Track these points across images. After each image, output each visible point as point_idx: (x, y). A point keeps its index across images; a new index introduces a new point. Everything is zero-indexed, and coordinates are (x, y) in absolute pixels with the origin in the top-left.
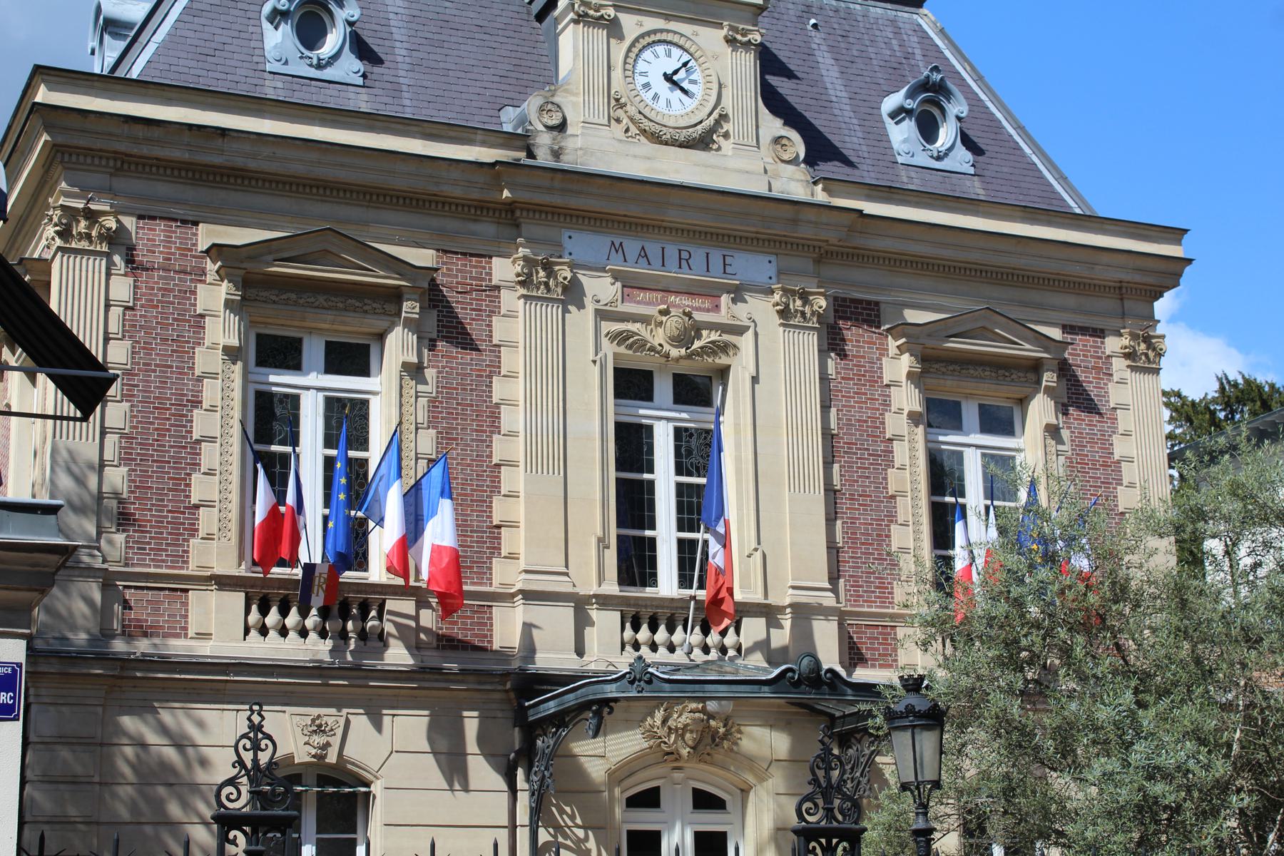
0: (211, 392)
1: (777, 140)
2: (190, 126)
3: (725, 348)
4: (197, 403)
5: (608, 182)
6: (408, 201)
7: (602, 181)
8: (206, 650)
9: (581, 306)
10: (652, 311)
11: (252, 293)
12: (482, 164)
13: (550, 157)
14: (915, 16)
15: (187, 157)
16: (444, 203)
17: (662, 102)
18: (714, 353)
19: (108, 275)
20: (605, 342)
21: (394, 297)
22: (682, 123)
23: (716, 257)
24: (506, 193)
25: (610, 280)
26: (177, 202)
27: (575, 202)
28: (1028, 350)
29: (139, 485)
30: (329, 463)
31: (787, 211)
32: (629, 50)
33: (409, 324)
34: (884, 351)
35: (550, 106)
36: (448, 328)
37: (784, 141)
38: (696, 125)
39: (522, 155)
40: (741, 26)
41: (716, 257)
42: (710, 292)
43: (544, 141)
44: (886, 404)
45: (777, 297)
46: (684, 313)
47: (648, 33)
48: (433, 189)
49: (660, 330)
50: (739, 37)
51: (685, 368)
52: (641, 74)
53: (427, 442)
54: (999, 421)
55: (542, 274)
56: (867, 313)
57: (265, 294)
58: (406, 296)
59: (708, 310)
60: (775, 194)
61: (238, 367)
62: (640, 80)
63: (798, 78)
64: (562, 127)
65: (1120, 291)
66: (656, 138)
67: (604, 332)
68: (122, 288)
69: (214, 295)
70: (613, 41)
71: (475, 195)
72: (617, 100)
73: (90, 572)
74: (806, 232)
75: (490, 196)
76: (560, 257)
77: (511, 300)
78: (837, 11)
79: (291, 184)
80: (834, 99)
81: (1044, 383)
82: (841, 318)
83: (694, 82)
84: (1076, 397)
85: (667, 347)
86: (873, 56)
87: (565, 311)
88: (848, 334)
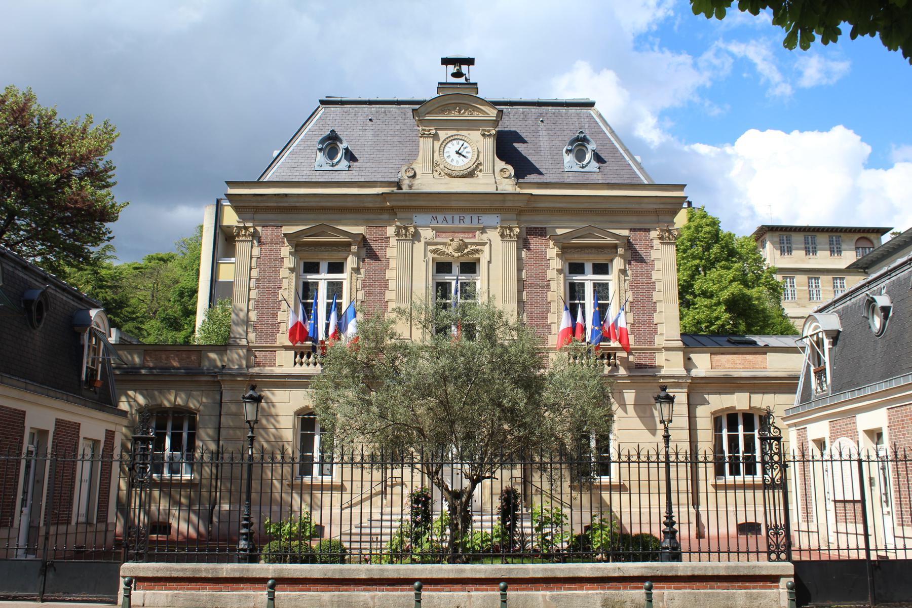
0: (285, 284)
1: (502, 170)
2: (275, 195)
3: (477, 251)
4: (280, 288)
8: (277, 371)
9: (419, 241)
10: (447, 240)
11: (299, 248)
18: (473, 254)
19: (252, 247)
20: (429, 253)
21: (349, 245)
27: (414, 204)
28: (610, 240)
29: (260, 317)
30: (329, 305)
31: (501, 198)
33: (354, 254)
36: (368, 252)
39: (395, 189)
42: (472, 231)
44: (548, 267)
51: (464, 260)
53: (361, 295)
54: (601, 269)
56: (541, 232)
60: (499, 192)
61: (294, 274)
62: (446, 155)
64: (414, 176)
65: (657, 212)
66: (450, 176)
68: (256, 252)
71: (378, 205)
73: (243, 347)
77: (393, 241)
84: (634, 256)
87: (413, 243)
88: (531, 241)
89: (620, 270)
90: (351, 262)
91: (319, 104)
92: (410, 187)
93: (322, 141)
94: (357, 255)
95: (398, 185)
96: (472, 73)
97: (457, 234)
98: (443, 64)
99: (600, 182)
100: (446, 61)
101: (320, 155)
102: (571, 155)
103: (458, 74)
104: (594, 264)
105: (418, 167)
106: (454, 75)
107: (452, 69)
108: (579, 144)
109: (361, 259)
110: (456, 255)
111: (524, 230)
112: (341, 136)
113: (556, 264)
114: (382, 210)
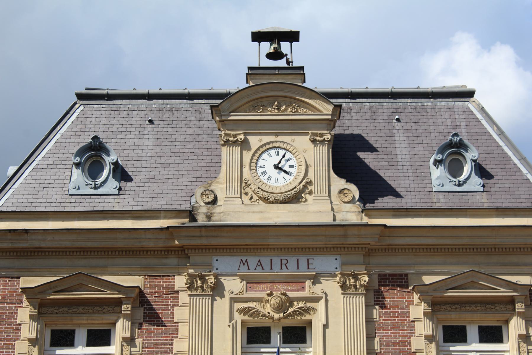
1: (341, 191)
2: (10, 231)
3: (307, 310)
5: (231, 229)
6: (128, 253)
7: (228, 229)
9: (222, 296)
10: (263, 295)
11: (44, 310)
12: (161, 229)
13: (205, 219)
14: (466, 103)
15: (10, 245)
16: (147, 251)
17: (273, 180)
18: (301, 314)
20: (237, 314)
21: (118, 303)
22: (283, 190)
23: (303, 261)
24: (177, 242)
25: (239, 280)
26: (9, 268)
27: (214, 242)
28: (503, 292)
31: (341, 231)
32: (253, 155)
33: (126, 317)
34: (411, 302)
35: (207, 192)
37: (346, 191)
38: (292, 190)
39: (186, 221)
40: (319, 132)
41: (303, 261)
43: (202, 211)
45: (338, 279)
46: (282, 294)
47: (265, 145)
48: (139, 245)
49: (268, 305)
50: (318, 138)
51: (288, 323)
52: (261, 167)
55: (199, 282)
56: (400, 281)
57: (51, 309)
58: (124, 303)
59: (298, 291)
60: (337, 222)
62: (260, 170)
63: (377, 151)
64: (214, 202)
66: (266, 200)
67: (236, 309)
69: (24, 313)
70: (244, 152)
71: (161, 244)
72: (246, 183)
74: (352, 241)
75: (170, 244)
76: (210, 271)
77: (184, 297)
78: (415, 108)
79: (66, 252)
80: (400, 160)
81: (517, 310)
82: (382, 285)
83: (291, 167)
85: (272, 313)
86: (432, 131)
87: (213, 300)
88: (386, 294)
89: (520, 336)
90: (121, 329)
91: (75, 99)
92: (209, 217)
93: (80, 153)
94: (131, 318)
95: (191, 215)
96: (297, 53)
97: (277, 286)
98: (253, 40)
99: (486, 206)
100: (258, 37)
101: (77, 173)
102: (441, 168)
103: (276, 55)
104: (480, 327)
105: (220, 189)
106: (270, 56)
107: (267, 47)
108: (453, 153)
109: (136, 324)
110: (276, 316)
111: (376, 277)
112: (107, 145)
113: (424, 328)
114: (168, 251)
